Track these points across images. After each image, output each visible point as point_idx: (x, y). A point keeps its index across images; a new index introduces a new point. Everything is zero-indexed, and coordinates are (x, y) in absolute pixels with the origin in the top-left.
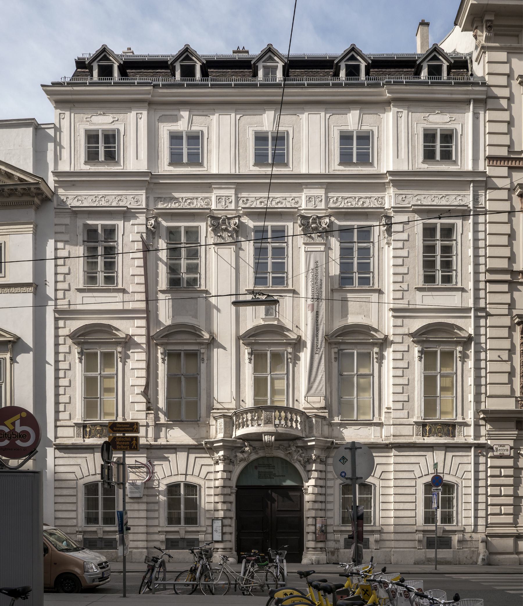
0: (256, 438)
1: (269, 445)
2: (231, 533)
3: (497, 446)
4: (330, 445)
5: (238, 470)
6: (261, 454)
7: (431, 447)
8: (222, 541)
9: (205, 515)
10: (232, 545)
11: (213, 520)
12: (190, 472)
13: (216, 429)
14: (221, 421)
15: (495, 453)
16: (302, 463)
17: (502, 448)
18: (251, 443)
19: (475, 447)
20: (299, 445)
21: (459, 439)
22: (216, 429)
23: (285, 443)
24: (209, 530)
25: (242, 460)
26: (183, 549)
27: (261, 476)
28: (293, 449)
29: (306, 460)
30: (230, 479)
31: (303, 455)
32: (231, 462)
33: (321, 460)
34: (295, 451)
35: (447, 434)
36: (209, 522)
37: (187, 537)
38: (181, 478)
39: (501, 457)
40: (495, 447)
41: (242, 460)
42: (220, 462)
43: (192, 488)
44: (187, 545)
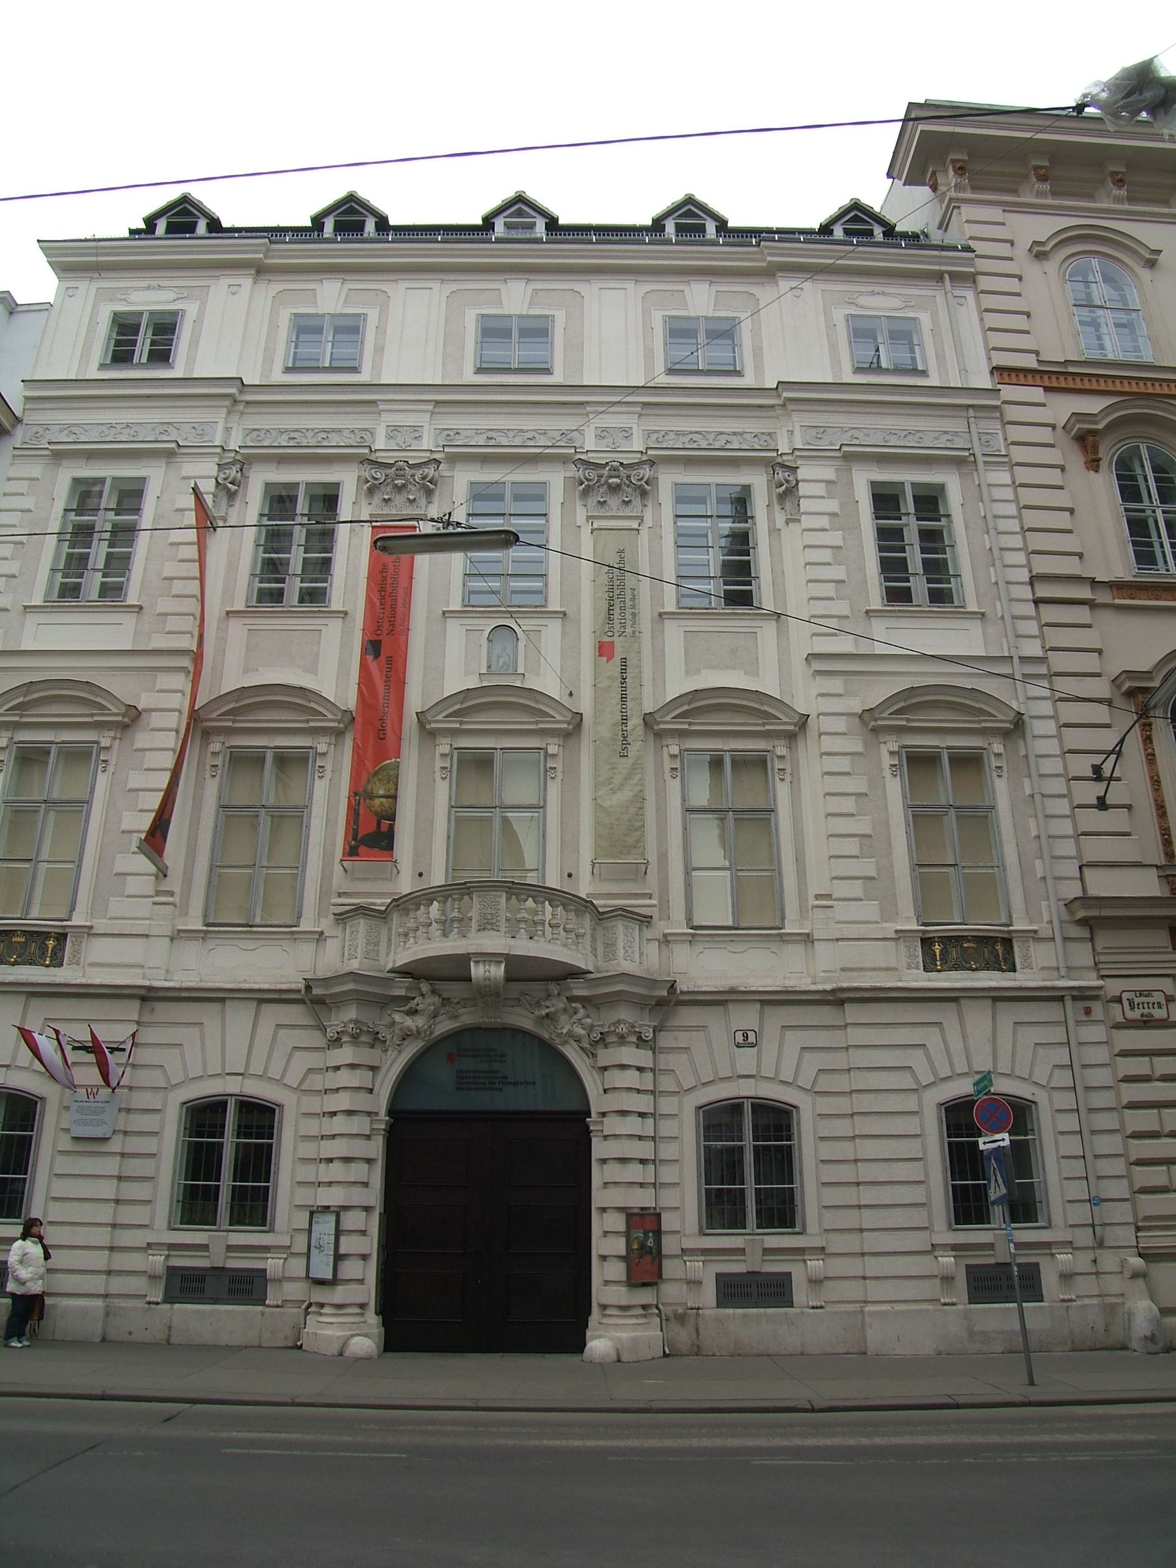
1: (488, 995)
6: (468, 1018)
11: (312, 1213)
15: (1130, 1015)
16: (586, 1045)
18: (440, 985)
21: (1024, 978)
23: (537, 989)
24: (300, 1245)
25: (406, 1036)
28: (561, 1004)
31: (589, 1020)
32: (376, 1039)
33: (640, 1038)
34: (565, 1010)
35: (993, 964)
36: (302, 1220)
37: (232, 1264)
39: (1147, 1023)
40: (1125, 996)
41: (406, 1036)
42: (345, 1039)
44: (231, 1291)
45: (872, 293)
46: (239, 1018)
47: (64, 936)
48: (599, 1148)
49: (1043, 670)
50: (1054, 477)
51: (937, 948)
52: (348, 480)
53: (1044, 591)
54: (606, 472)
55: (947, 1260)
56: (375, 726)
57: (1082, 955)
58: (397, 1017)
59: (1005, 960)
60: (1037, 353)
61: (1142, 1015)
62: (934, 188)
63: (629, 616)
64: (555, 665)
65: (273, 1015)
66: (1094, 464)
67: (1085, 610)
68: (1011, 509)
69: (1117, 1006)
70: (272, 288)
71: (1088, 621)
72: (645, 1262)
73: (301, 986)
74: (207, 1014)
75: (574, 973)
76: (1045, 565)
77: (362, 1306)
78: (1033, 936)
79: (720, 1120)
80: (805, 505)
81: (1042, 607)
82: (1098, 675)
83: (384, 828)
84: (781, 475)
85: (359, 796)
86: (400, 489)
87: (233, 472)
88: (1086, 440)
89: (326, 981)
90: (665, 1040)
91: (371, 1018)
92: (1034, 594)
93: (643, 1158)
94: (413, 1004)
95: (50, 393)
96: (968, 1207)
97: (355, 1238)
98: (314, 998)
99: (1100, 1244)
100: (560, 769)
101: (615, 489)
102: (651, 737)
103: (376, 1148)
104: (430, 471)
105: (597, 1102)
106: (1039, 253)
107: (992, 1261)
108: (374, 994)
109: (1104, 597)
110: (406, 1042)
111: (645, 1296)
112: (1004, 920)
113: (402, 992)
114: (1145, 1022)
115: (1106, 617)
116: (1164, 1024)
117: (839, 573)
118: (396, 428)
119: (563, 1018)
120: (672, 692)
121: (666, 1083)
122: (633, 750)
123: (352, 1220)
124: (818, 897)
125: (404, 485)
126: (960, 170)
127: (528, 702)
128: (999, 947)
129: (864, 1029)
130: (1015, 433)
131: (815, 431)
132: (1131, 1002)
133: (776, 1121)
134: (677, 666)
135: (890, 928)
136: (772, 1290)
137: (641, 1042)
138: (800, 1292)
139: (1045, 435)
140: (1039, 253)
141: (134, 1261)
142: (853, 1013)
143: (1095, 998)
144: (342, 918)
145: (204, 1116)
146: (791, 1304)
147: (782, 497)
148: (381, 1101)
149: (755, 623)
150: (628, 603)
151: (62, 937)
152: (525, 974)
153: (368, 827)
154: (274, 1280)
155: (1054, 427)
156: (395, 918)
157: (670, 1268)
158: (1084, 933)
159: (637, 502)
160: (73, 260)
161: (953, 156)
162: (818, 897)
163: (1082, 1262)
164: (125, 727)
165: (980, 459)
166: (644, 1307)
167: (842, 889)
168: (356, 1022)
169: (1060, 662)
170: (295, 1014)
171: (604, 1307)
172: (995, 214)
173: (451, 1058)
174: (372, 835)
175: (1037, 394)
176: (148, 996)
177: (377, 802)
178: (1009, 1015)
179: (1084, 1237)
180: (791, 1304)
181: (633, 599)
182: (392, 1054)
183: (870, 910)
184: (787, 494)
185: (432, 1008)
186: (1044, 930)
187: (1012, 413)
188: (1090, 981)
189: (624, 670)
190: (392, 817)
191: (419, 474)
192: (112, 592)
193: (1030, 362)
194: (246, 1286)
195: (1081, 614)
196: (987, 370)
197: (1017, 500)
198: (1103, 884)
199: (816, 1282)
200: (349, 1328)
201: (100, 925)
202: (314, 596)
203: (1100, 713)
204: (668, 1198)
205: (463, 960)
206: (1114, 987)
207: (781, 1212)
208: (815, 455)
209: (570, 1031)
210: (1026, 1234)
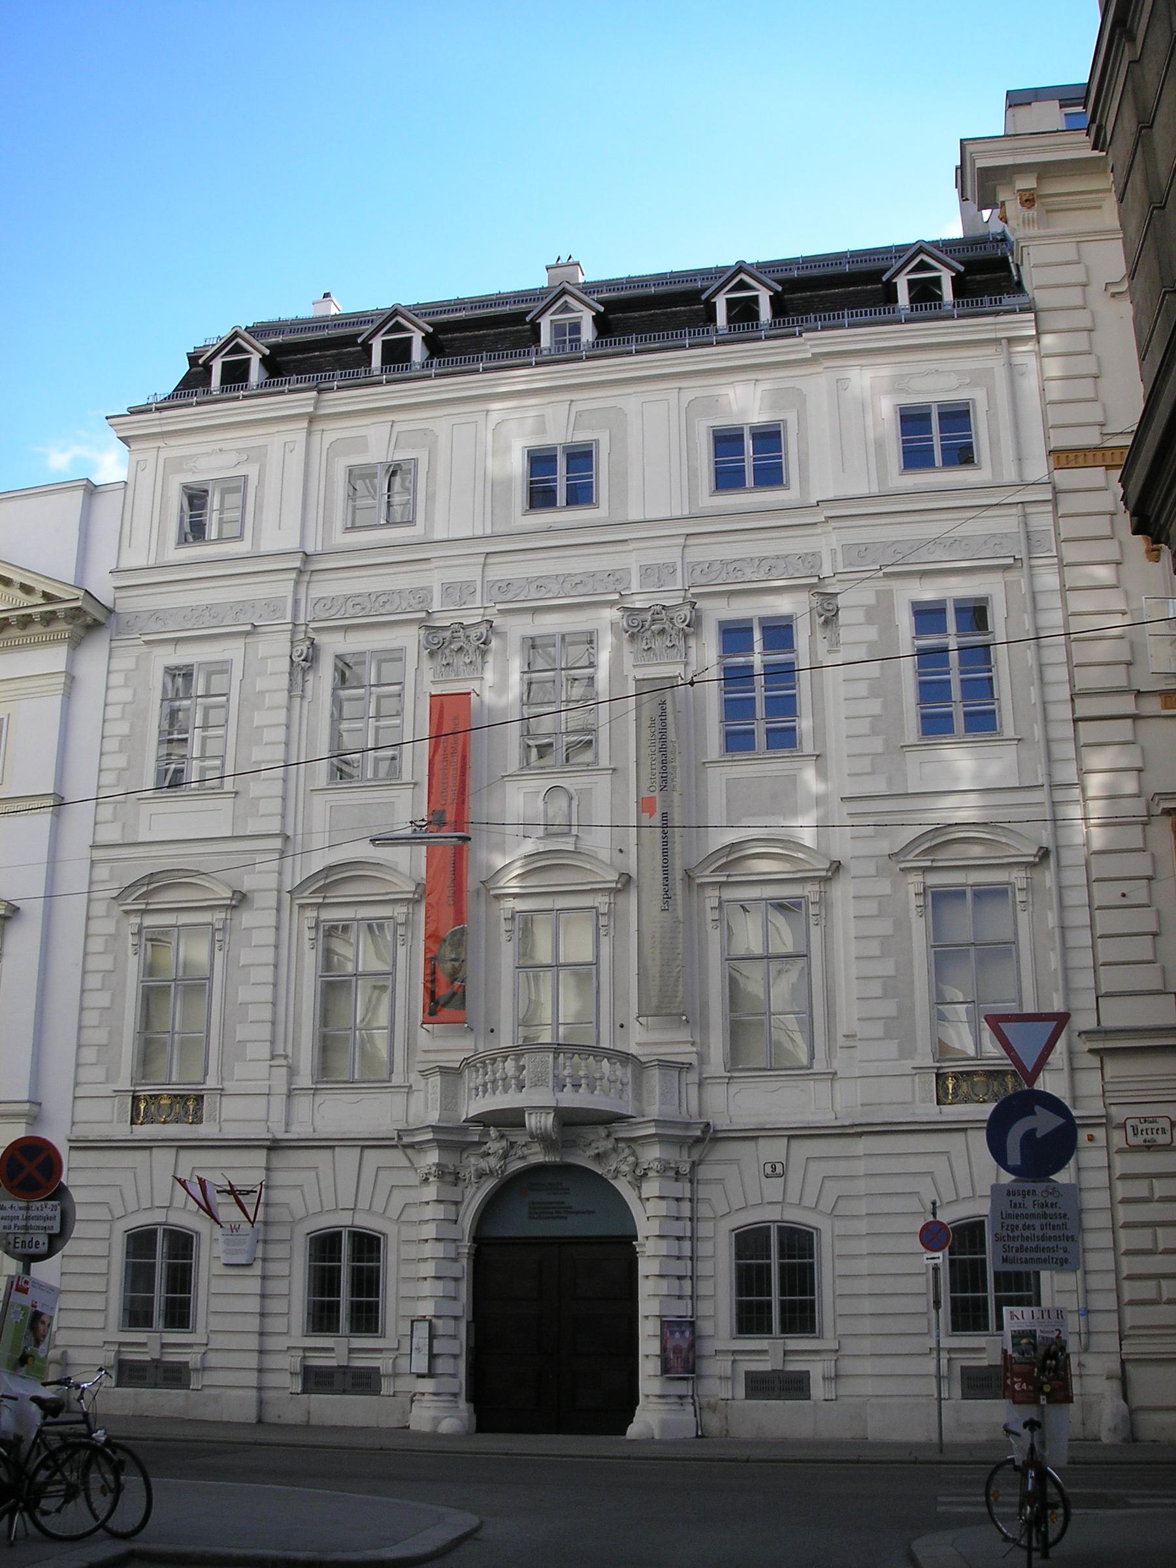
0: (511, 1120)
2: (455, 1357)
4: (698, 1133)
5: (475, 1198)
8: (430, 1374)
9: (397, 1309)
10: (460, 1383)
12: (363, 1204)
13: (426, 1098)
14: (436, 1080)
15: (1133, 1140)
17: (1151, 1125)
18: (506, 1131)
22: (426, 1098)
26: (344, 1392)
29: (638, 1172)
30: (456, 1222)
33: (677, 1173)
34: (615, 1149)
39: (1149, 1147)
41: (481, 1175)
43: (368, 1245)
58: (473, 1160)
61: (1145, 1141)
72: (683, 1362)
90: (704, 1172)
91: (451, 1161)
94: (484, 1148)
98: (402, 1142)
108: (453, 1140)
110: (483, 1180)
111: (683, 1388)
113: (476, 1139)
114: (1149, 1147)
116: (1167, 1148)
133: (799, 1243)
135: (908, 1065)
136: (793, 1386)
138: (818, 1389)
146: (808, 1397)
149: (795, 765)
151: (199, 1099)
166: (681, 1397)
168: (438, 1165)
180: (808, 1397)
183: (891, 1048)
185: (501, 1151)
198: (1118, 1015)
207: (801, 1318)
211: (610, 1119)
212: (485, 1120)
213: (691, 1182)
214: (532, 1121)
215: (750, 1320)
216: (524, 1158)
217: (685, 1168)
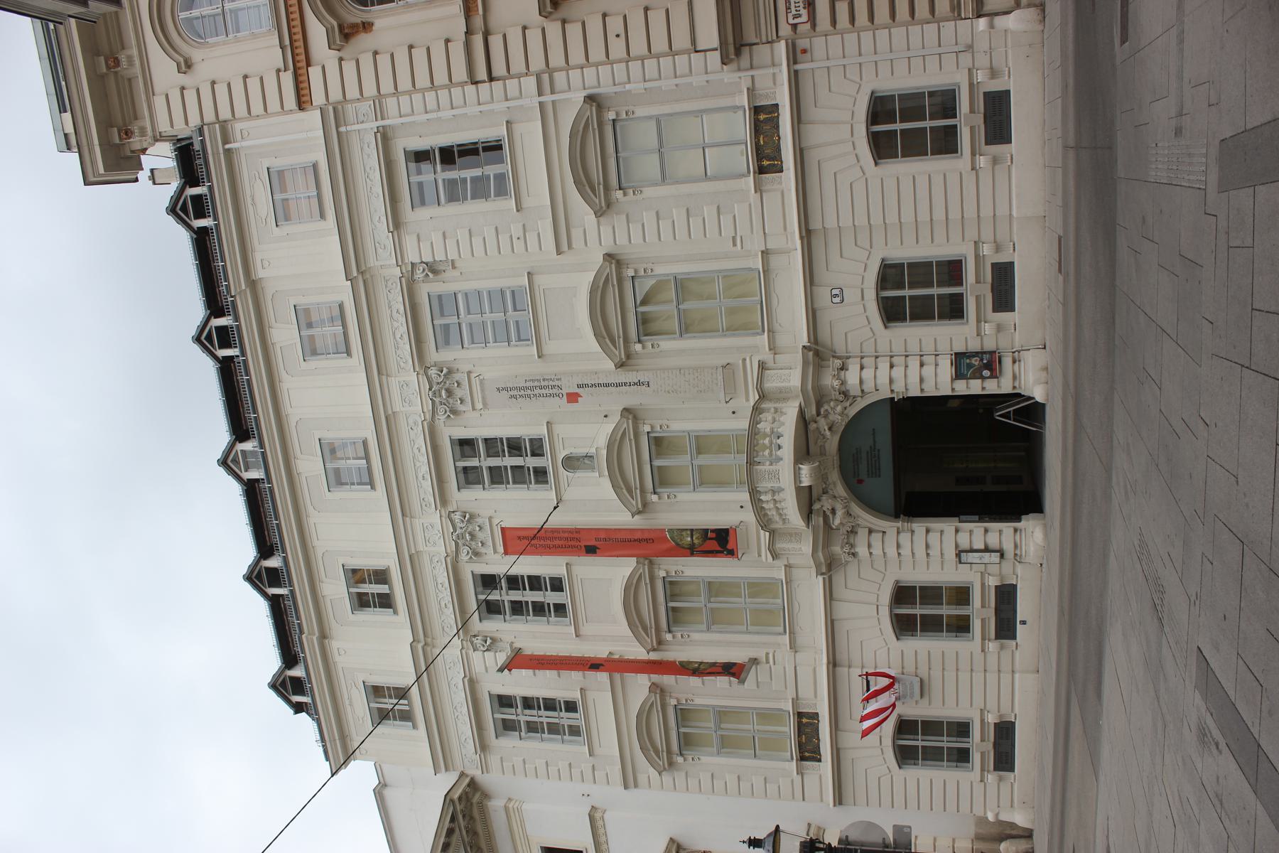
2: (986, 531)
3: (790, 16)
5: (866, 518)
6: (835, 476)
7: (800, 155)
15: (804, 18)
19: (795, 62)
20: (814, 412)
25: (849, 514)
27: (875, 471)
29: (841, 398)
34: (826, 417)
38: (885, 612)
40: (791, 21)
41: (849, 514)
45: (254, 204)
46: (842, 610)
47: (799, 714)
48: (914, 392)
49: (546, 77)
50: (384, 61)
51: (765, 163)
52: (470, 569)
53: (482, 74)
54: (437, 400)
55: (982, 161)
56: (643, 544)
57: (762, 52)
58: (837, 522)
59: (770, 113)
60: (278, 71)
62: (144, 151)
63: (546, 383)
64: (588, 431)
65: (839, 591)
66: (367, 26)
67: (491, 38)
68: (417, 97)
69: (800, 28)
70: (335, 628)
71: (500, 36)
73: (820, 578)
74: (841, 629)
75: (802, 413)
76: (460, 73)
77: (1016, 530)
78: (751, 91)
79: (892, 312)
80: (440, 256)
81: (494, 74)
82: (543, 30)
83: (714, 535)
84: (419, 275)
85: (692, 551)
86: (473, 536)
87: (478, 641)
88: (346, 33)
89: (818, 566)
91: (839, 538)
92: (484, 82)
93: (919, 363)
94: (828, 513)
95: (442, 757)
96: (946, 143)
97: (974, 538)
98: (829, 567)
99: (970, 48)
100: (660, 422)
101: (450, 393)
102: (631, 362)
103: (919, 526)
104: (457, 517)
105: (887, 394)
106: (186, 66)
107: (982, 127)
109: (478, 21)
111: (1007, 362)
112: (741, 113)
113: (821, 519)
115: (494, 22)
117: (489, 233)
118: (426, 541)
119: (831, 417)
120: (595, 347)
121: (869, 349)
122: (642, 377)
123: (964, 541)
124: (735, 245)
125: (470, 534)
126: (128, 133)
127: (615, 446)
128: (762, 117)
129: (828, 216)
130: (352, 92)
131: (380, 251)
132: (795, 17)
134: (576, 343)
137: (843, 368)
139: (349, 67)
140: (186, 66)
141: (992, 660)
142: (816, 224)
143: (794, 45)
144: (775, 556)
145: (904, 626)
147: (435, 272)
148: (890, 526)
150: (536, 384)
151: (800, 715)
152: (804, 452)
153: (714, 545)
154: (1002, 579)
155: (341, 59)
156: (773, 526)
157: (989, 345)
158: (746, 50)
159: (457, 376)
160: (339, 752)
161: (117, 141)
162: (735, 245)
163: (982, 61)
164: (662, 691)
165: (380, 123)
166: (1014, 362)
167: (728, 231)
169: (537, 63)
170: (838, 579)
171: (1014, 388)
172: (159, 102)
173: (860, 482)
174: (720, 542)
175: (315, 72)
176: (833, 663)
177: (696, 541)
178: (810, 112)
179: (966, 59)
181: (533, 381)
182: (860, 522)
184: (433, 269)
186: (745, 84)
187: (335, 95)
188: (781, 47)
189: (587, 385)
190: (706, 531)
191: (459, 525)
192: (571, 707)
193: (287, 78)
194: (1006, 595)
195: (496, 42)
196: (302, 115)
197: (409, 93)
199: (998, 248)
200: (1032, 536)
201: (791, 694)
202: (557, 585)
203: (574, 30)
204: (944, 347)
205: (799, 490)
206: (785, 30)
208: (399, 249)
209: (839, 414)
210: (964, 105)
211: (803, 422)
212: (808, 512)
213: (848, 358)
214: (806, 482)
215: (954, 309)
216: (834, 484)
217: (838, 363)
